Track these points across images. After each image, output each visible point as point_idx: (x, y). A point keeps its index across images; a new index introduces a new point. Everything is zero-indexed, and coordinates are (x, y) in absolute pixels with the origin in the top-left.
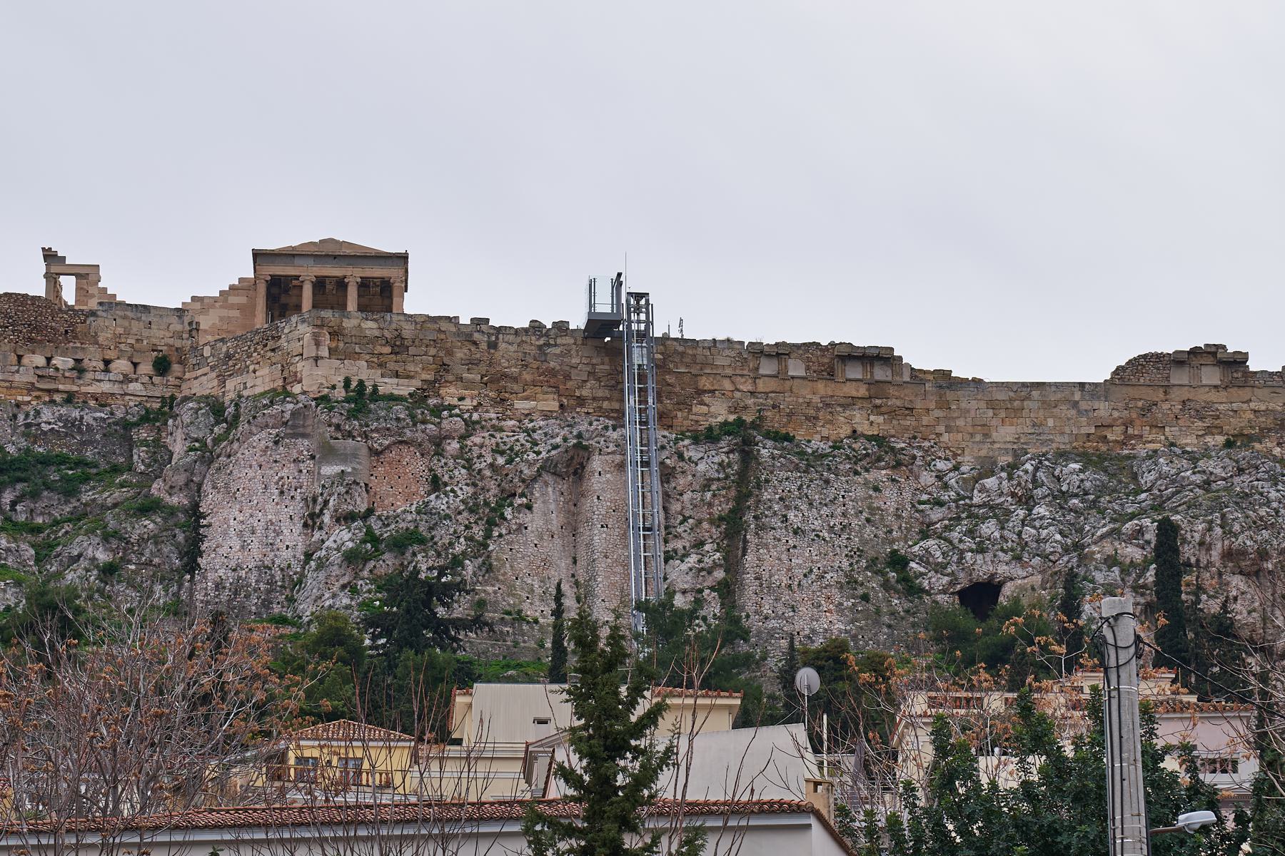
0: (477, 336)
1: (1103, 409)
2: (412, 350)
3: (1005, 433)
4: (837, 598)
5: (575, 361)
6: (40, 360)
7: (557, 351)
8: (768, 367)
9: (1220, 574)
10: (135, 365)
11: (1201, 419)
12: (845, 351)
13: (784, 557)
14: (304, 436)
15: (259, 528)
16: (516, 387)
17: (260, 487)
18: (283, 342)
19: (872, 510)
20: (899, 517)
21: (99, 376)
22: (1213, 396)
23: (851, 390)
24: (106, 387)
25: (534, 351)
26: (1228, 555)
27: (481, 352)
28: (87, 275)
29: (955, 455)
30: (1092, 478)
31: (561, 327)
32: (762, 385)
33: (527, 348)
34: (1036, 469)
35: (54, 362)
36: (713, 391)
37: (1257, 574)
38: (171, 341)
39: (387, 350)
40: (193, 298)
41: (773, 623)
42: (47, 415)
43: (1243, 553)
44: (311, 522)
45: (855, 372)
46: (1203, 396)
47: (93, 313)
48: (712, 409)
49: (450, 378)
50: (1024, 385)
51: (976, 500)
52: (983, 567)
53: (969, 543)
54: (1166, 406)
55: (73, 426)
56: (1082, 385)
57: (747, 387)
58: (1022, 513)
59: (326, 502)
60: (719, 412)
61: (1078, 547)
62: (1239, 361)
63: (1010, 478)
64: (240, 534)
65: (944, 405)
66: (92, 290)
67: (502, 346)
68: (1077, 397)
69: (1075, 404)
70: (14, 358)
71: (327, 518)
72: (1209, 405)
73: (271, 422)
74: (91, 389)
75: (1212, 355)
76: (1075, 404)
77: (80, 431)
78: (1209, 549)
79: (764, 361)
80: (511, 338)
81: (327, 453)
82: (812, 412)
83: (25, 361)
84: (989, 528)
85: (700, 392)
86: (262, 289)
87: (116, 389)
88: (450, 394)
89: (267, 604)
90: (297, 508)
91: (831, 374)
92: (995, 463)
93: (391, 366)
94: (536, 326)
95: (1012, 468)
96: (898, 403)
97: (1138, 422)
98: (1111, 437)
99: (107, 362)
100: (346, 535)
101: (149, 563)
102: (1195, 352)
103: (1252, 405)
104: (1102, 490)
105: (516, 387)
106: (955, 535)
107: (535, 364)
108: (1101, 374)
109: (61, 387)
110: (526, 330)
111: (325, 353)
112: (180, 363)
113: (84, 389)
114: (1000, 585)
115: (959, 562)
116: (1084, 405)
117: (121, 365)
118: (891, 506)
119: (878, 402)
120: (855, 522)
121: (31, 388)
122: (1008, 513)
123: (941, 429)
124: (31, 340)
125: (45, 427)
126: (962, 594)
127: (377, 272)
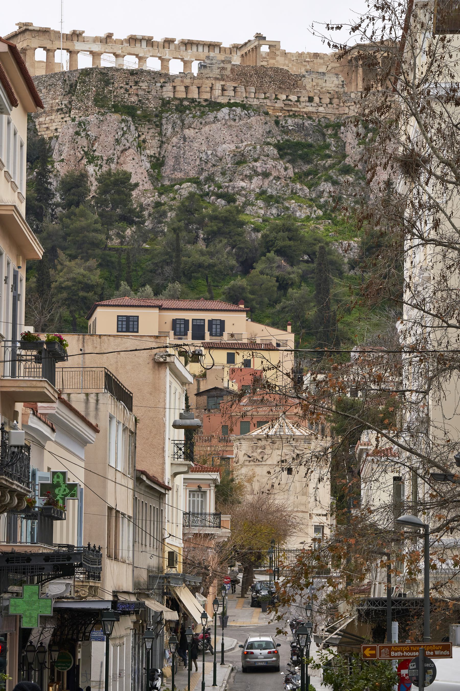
6: (284, 97)
10: (320, 99)
21: (308, 104)
24: (310, 109)
35: (290, 98)
38: (334, 89)
42: (290, 121)
55: (301, 127)
77: (303, 130)
87: (314, 110)
101: (351, 195)
109: (293, 109)
112: (338, 98)
113: (302, 110)
117: (316, 99)
121: (282, 109)
124: (280, 88)
125: (290, 128)
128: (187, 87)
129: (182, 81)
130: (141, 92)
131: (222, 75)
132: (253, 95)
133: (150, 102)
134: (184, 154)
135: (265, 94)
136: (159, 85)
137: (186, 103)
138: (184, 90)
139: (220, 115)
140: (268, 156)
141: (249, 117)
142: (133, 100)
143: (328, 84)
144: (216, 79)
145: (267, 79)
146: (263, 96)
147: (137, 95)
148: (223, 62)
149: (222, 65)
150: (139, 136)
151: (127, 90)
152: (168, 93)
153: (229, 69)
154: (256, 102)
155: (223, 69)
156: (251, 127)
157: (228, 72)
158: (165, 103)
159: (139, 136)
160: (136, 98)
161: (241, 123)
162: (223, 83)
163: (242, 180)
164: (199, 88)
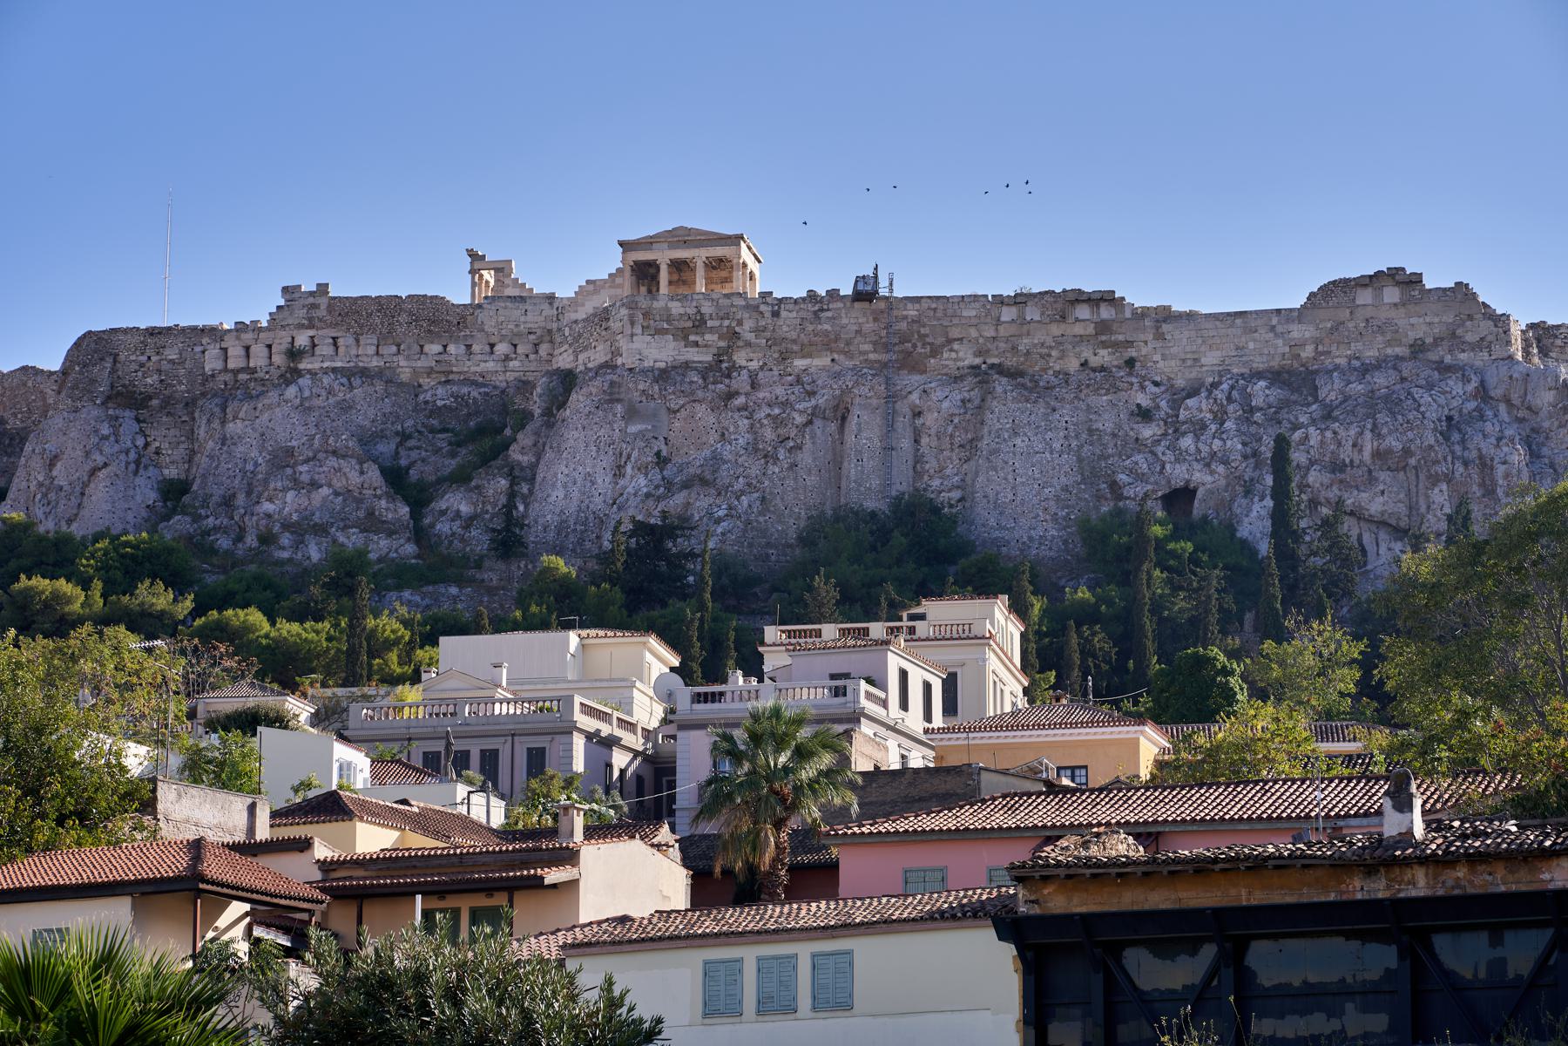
0: (763, 308)
1: (1297, 332)
2: (710, 323)
3: (1211, 359)
4: (1053, 510)
5: (845, 321)
7: (829, 314)
8: (1008, 314)
9: (1370, 471)
11: (1383, 334)
12: (1072, 297)
13: (1010, 477)
14: (618, 401)
15: (579, 481)
16: (795, 348)
17: (582, 446)
18: (611, 323)
19: (1091, 431)
20: (1114, 435)
22: (1393, 313)
23: (1078, 329)
24: (491, 365)
25: (810, 316)
26: (1377, 454)
27: (767, 320)
28: (502, 269)
29: (1169, 379)
30: (1276, 394)
31: (833, 294)
32: (1003, 331)
33: (803, 314)
34: (1232, 388)
36: (961, 339)
37: (1404, 468)
39: (690, 324)
40: (588, 282)
41: (997, 534)
42: (440, 391)
43: (1389, 451)
44: (619, 472)
45: (1083, 312)
46: (1384, 314)
47: (480, 306)
48: (961, 354)
49: (740, 343)
50: (1229, 314)
51: (1181, 417)
52: (1178, 474)
53: (1169, 456)
54: (1351, 325)
56: (1279, 311)
57: (989, 332)
58: (1213, 427)
59: (629, 457)
60: (966, 357)
61: (1255, 454)
62: (1416, 279)
63: (1208, 398)
64: (565, 486)
65: (1159, 336)
66: (507, 281)
67: (784, 314)
68: (1274, 322)
69: (1273, 328)
70: (417, 348)
71: (629, 469)
72: (1389, 322)
73: (594, 391)
74: (478, 369)
75: (1395, 276)
76: (1273, 328)
78: (1360, 451)
79: (1005, 309)
80: (791, 307)
81: (632, 414)
82: (1045, 351)
83: (427, 348)
84: (1187, 442)
85: (950, 341)
86: (628, 273)
88: (740, 358)
89: (581, 541)
90: (607, 461)
91: (1063, 317)
92: (1202, 385)
93: (692, 338)
94: (812, 295)
95: (1215, 385)
96: (1121, 338)
97: (1327, 341)
98: (1303, 355)
99: (492, 346)
100: (642, 481)
102: (1379, 274)
103: (1428, 319)
104: (1285, 404)
105: (795, 348)
106: (1159, 450)
107: (810, 328)
108: (1297, 301)
110: (804, 299)
111: (638, 330)
114: (1194, 491)
115: (1161, 472)
116: (1279, 329)
117: (502, 348)
118: (1109, 427)
119: (1104, 338)
120: (1074, 443)
122: (1204, 427)
123: (1157, 357)
125: (440, 403)
126: (1164, 497)
127: (719, 251)
128: (247, 349)
129: (238, 338)
130: (165, 366)
131: (310, 319)
132: (371, 350)
133: (180, 383)
134: (217, 467)
135: (398, 346)
136: (198, 349)
137: (243, 377)
138: (242, 352)
139: (291, 391)
140: (334, 453)
141: (351, 388)
142: (149, 380)
143: (530, 317)
144: (301, 326)
145: (404, 318)
146: (394, 348)
147: (159, 371)
148: (311, 294)
149: (311, 300)
150: (147, 445)
151: (142, 365)
152: (212, 363)
153: (323, 307)
154: (375, 363)
155: (314, 306)
156: (350, 407)
157: (322, 312)
158: (207, 379)
159: (147, 445)
160: (156, 377)
161: (332, 400)
162: (311, 333)
163: (270, 500)
164: (269, 347)
